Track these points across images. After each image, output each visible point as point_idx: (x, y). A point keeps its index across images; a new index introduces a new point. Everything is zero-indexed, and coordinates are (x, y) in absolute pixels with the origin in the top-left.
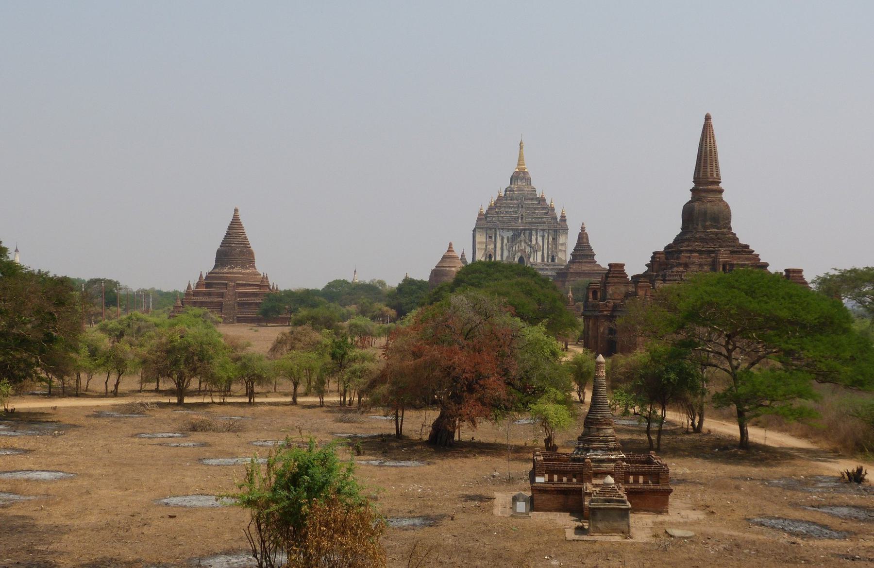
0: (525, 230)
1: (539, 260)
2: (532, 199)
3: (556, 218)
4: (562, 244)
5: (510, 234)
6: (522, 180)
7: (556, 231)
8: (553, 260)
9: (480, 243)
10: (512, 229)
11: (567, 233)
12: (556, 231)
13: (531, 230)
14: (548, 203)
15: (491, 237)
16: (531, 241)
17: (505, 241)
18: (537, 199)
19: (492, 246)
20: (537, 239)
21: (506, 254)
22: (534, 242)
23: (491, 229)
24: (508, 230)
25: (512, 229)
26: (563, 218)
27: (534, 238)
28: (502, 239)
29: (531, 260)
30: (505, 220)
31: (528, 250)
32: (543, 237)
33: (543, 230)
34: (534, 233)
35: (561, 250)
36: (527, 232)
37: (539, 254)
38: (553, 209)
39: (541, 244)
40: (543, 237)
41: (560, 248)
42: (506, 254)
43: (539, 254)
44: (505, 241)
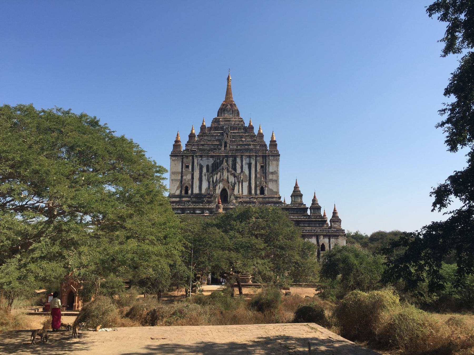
0: (227, 156)
1: (245, 192)
2: (240, 129)
3: (266, 145)
4: (272, 173)
7: (264, 157)
8: (262, 192)
10: (212, 157)
11: (278, 160)
12: (264, 157)
14: (256, 132)
15: (187, 167)
16: (235, 169)
17: (204, 170)
18: (246, 129)
19: (189, 177)
20: (242, 165)
21: (205, 185)
22: (239, 171)
23: (187, 157)
24: (208, 157)
25: (212, 157)
26: (273, 143)
27: (238, 166)
29: (236, 192)
30: (206, 147)
31: (232, 179)
33: (250, 157)
34: (238, 160)
35: (272, 180)
36: (230, 160)
37: (246, 185)
38: (261, 135)
39: (247, 172)
41: (271, 177)
42: (205, 185)
44: (204, 170)
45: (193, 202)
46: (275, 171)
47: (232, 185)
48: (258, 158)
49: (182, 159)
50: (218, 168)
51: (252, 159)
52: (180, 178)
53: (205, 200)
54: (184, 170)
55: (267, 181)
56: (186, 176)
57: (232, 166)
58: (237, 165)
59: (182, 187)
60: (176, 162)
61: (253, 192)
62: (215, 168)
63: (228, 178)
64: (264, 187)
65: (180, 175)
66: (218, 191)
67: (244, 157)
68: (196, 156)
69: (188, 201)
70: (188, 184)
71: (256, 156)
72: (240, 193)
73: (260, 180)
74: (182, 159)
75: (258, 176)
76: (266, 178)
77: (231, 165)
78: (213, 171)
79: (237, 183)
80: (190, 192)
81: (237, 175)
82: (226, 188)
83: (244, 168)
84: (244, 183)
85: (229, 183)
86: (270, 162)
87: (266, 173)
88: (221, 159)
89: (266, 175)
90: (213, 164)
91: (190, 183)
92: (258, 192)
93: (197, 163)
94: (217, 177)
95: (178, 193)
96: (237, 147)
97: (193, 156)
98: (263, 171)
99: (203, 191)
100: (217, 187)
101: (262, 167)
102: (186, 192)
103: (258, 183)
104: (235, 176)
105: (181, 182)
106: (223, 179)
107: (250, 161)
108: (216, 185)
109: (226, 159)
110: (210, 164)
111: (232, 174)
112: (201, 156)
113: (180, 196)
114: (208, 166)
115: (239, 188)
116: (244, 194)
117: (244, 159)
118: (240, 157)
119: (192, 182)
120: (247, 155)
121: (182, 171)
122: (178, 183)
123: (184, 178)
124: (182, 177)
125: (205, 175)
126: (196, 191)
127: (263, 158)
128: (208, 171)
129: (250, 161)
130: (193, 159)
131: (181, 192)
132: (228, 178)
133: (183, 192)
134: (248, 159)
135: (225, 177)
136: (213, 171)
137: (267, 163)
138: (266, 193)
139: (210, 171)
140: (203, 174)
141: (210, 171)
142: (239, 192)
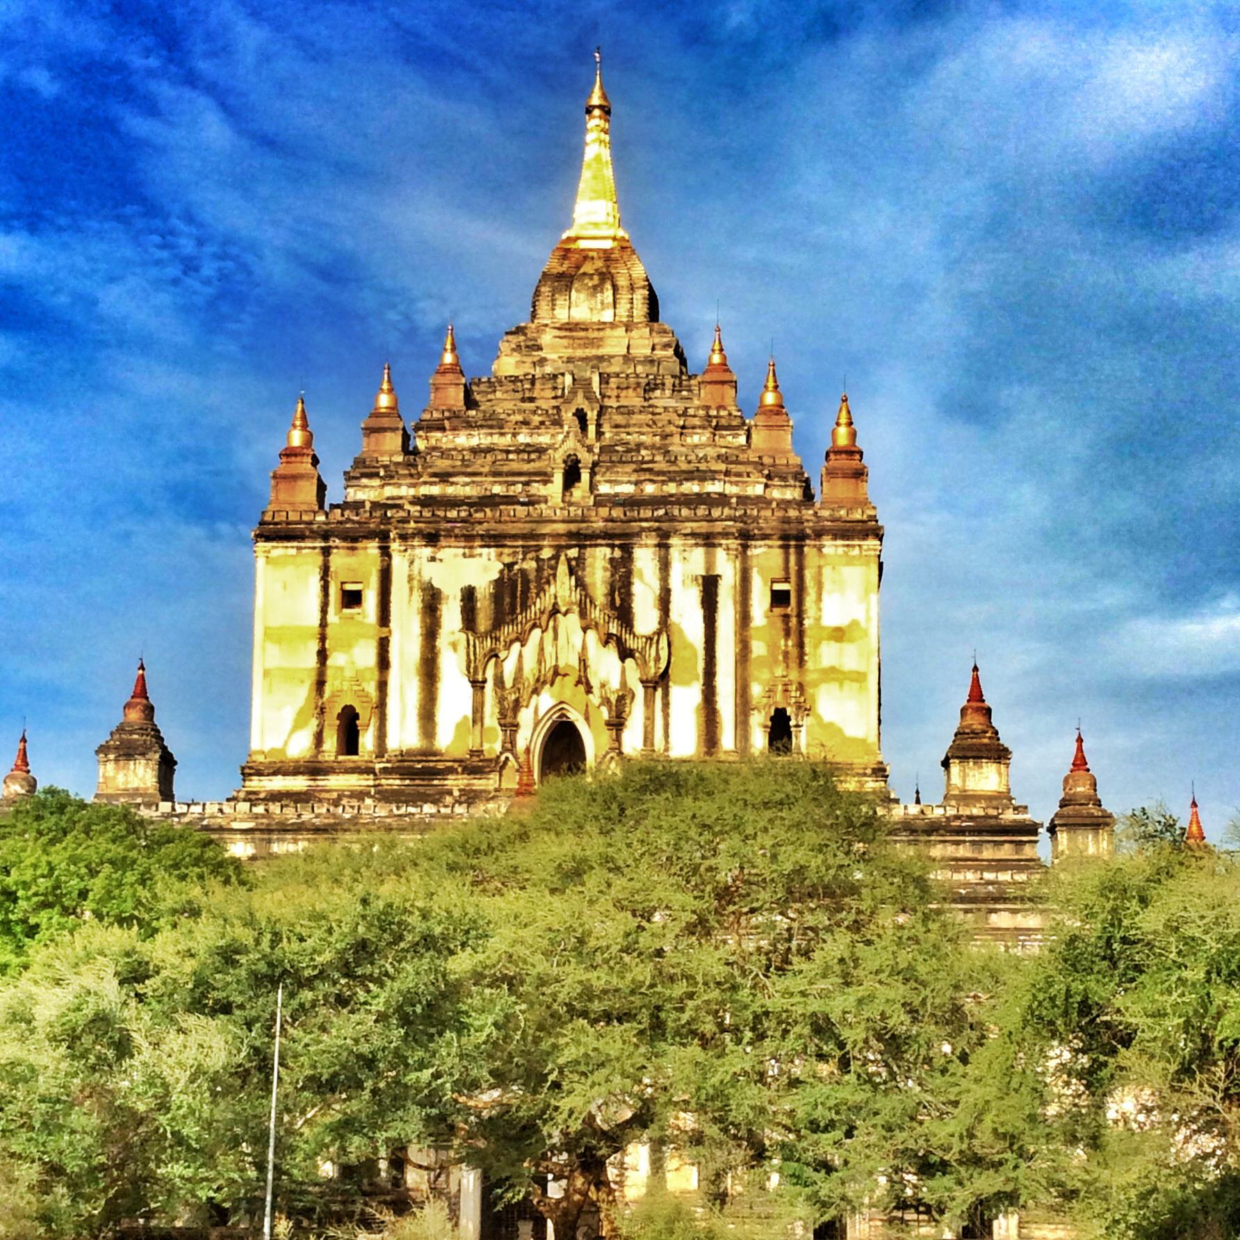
1: (684, 742)
4: (839, 634)
5: (480, 569)
6: (597, 289)
9: (276, 635)
10: (495, 540)
13: (623, 542)
15: (352, 599)
16: (623, 613)
17: (451, 615)
19: (367, 655)
22: (645, 618)
23: (353, 538)
28: (432, 602)
29: (632, 741)
31: (607, 668)
32: (709, 585)
33: (708, 541)
34: (645, 558)
35: (833, 674)
36: (599, 559)
37: (685, 696)
40: (709, 585)
43: (685, 696)
44: (451, 615)
45: (386, 796)
46: (854, 624)
47: (606, 701)
48: (758, 551)
49: (326, 552)
50: (525, 607)
51: (720, 554)
52: (312, 661)
53: (455, 783)
54: (332, 617)
55: (810, 677)
56: (347, 646)
57: (611, 594)
58: (637, 588)
59: (322, 711)
60: (289, 572)
61: (727, 739)
62: (512, 600)
63: (583, 661)
64: (789, 711)
65: (315, 646)
66: (530, 736)
67: (674, 541)
68: (403, 537)
69: (360, 795)
70: (361, 693)
71: (746, 537)
72: (659, 743)
73: (765, 675)
74: (326, 552)
75: (758, 648)
76: (801, 662)
77: (600, 591)
78: (498, 623)
79: (639, 691)
80: (367, 741)
81: (631, 643)
82: (575, 717)
83: (673, 607)
84: (675, 690)
85: (589, 690)
86: (827, 571)
87: (801, 634)
88: (546, 553)
89: (801, 645)
90: (498, 583)
91: (371, 688)
92: (759, 740)
93: (410, 579)
94: (521, 659)
95: (300, 747)
96: (637, 483)
97: (384, 537)
98: (786, 617)
99: (445, 739)
100: (525, 717)
101: (779, 599)
102: (350, 743)
103: (756, 690)
104: (625, 653)
105: (320, 684)
106: (556, 673)
107: (710, 564)
108: (517, 705)
109: (573, 553)
110: (484, 588)
111: (607, 639)
112: (432, 539)
113: (314, 769)
114: (469, 595)
115: (650, 719)
116: (675, 754)
117: (675, 554)
118: (652, 540)
119: (382, 686)
120: (693, 535)
121: (323, 624)
122: (303, 692)
123: (334, 660)
124: (323, 655)
125: (454, 646)
126: (403, 734)
127: (785, 548)
128: (469, 621)
129: (710, 564)
130: (385, 552)
131: (319, 739)
132: (583, 661)
133: (331, 743)
134: (699, 553)
135: (569, 659)
136: (498, 623)
137: (808, 574)
138: (803, 739)
139: (483, 623)
140: (442, 642)
141: (483, 623)
142: (648, 738)
